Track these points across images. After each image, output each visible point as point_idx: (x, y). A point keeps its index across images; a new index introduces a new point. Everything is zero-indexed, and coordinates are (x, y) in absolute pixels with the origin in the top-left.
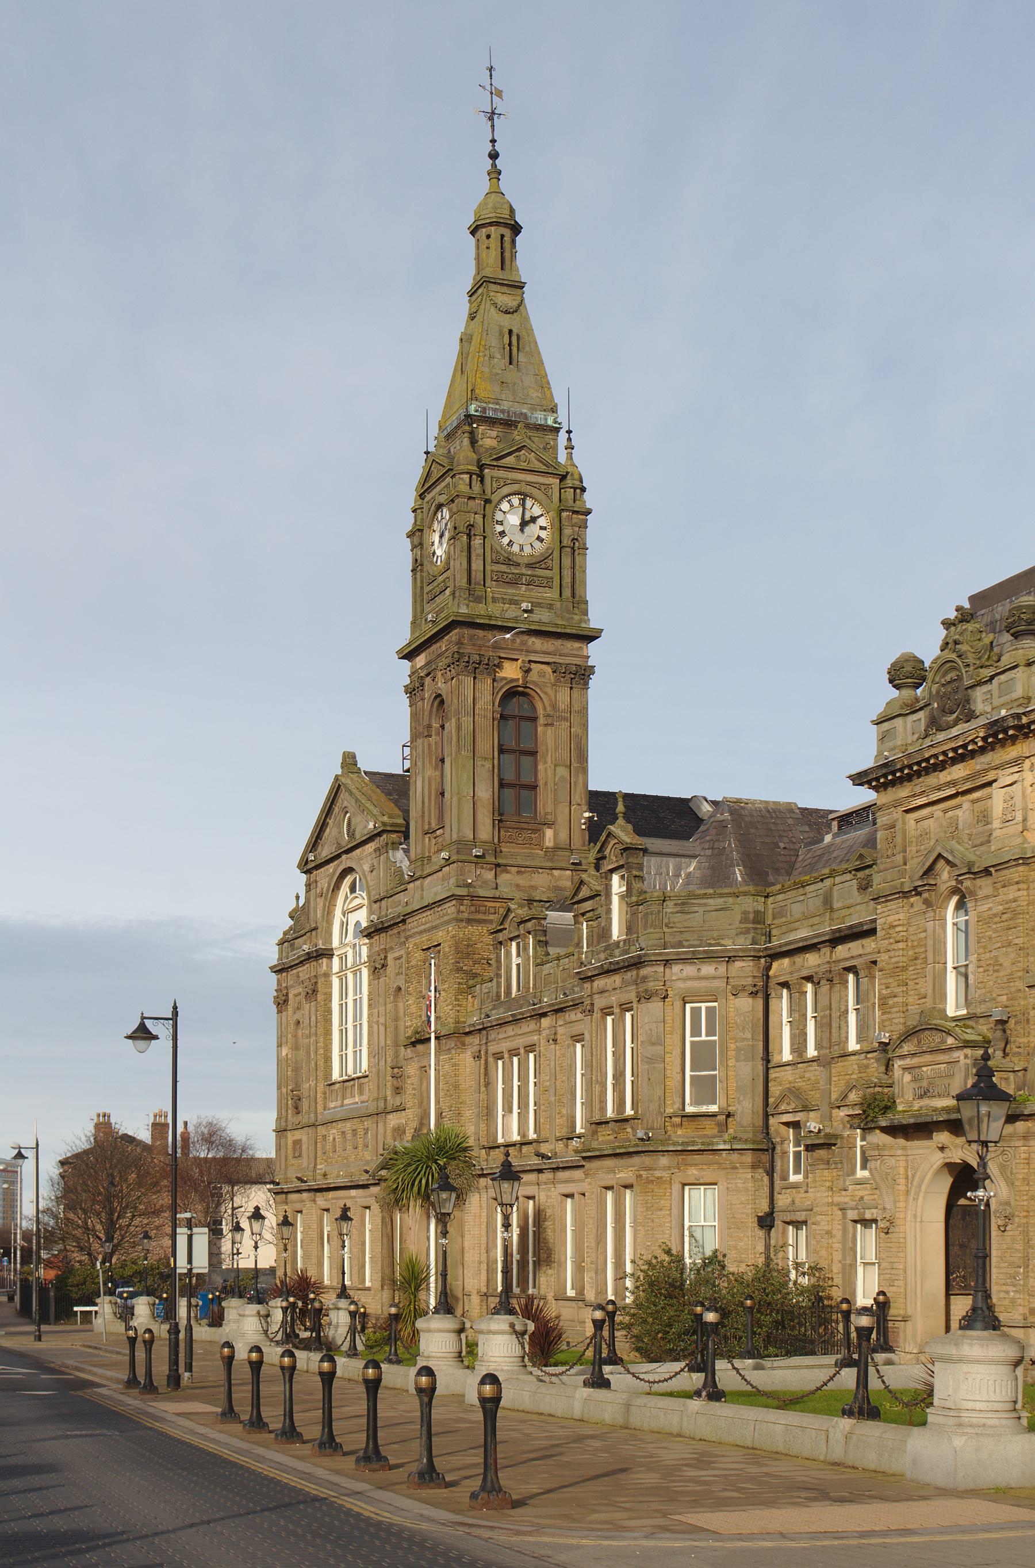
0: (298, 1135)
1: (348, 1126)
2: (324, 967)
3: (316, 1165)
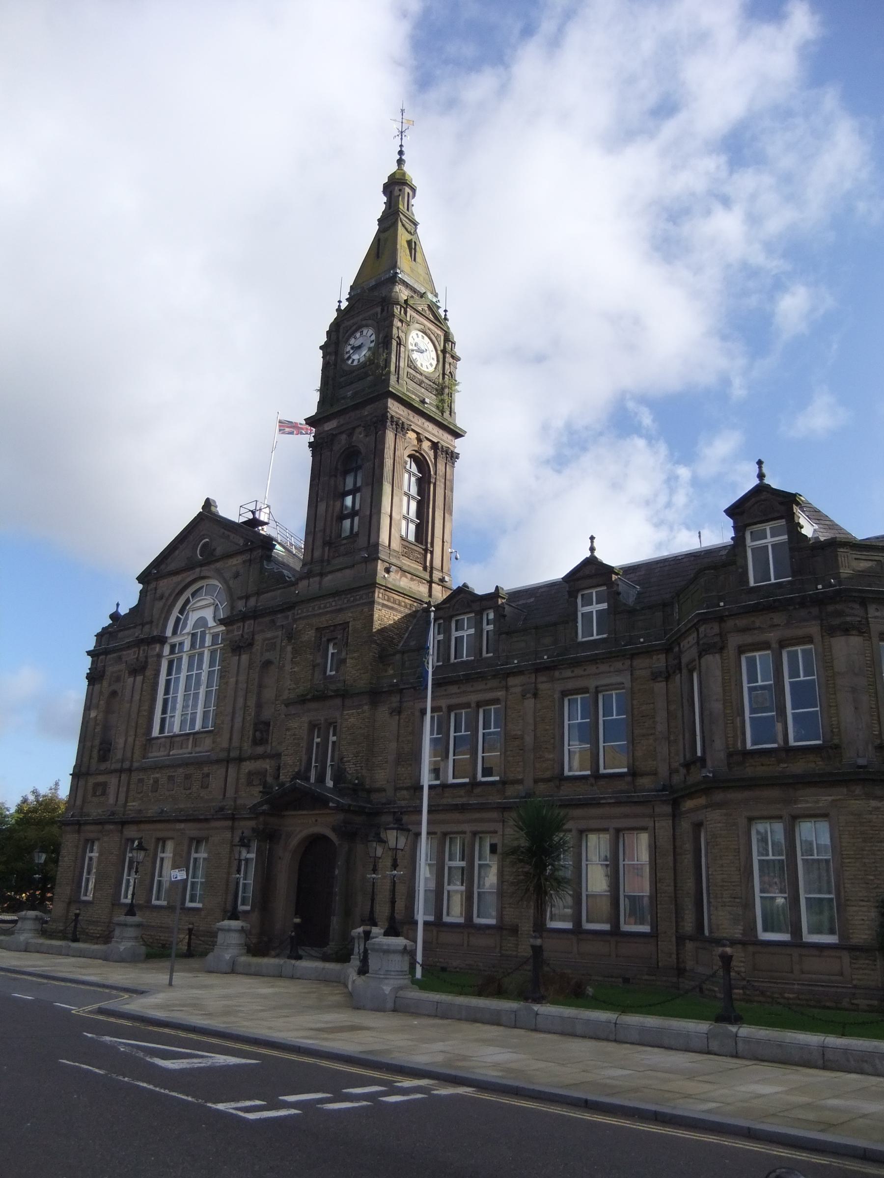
0: (101, 779)
1: (181, 770)
2: (157, 650)
3: (126, 801)
